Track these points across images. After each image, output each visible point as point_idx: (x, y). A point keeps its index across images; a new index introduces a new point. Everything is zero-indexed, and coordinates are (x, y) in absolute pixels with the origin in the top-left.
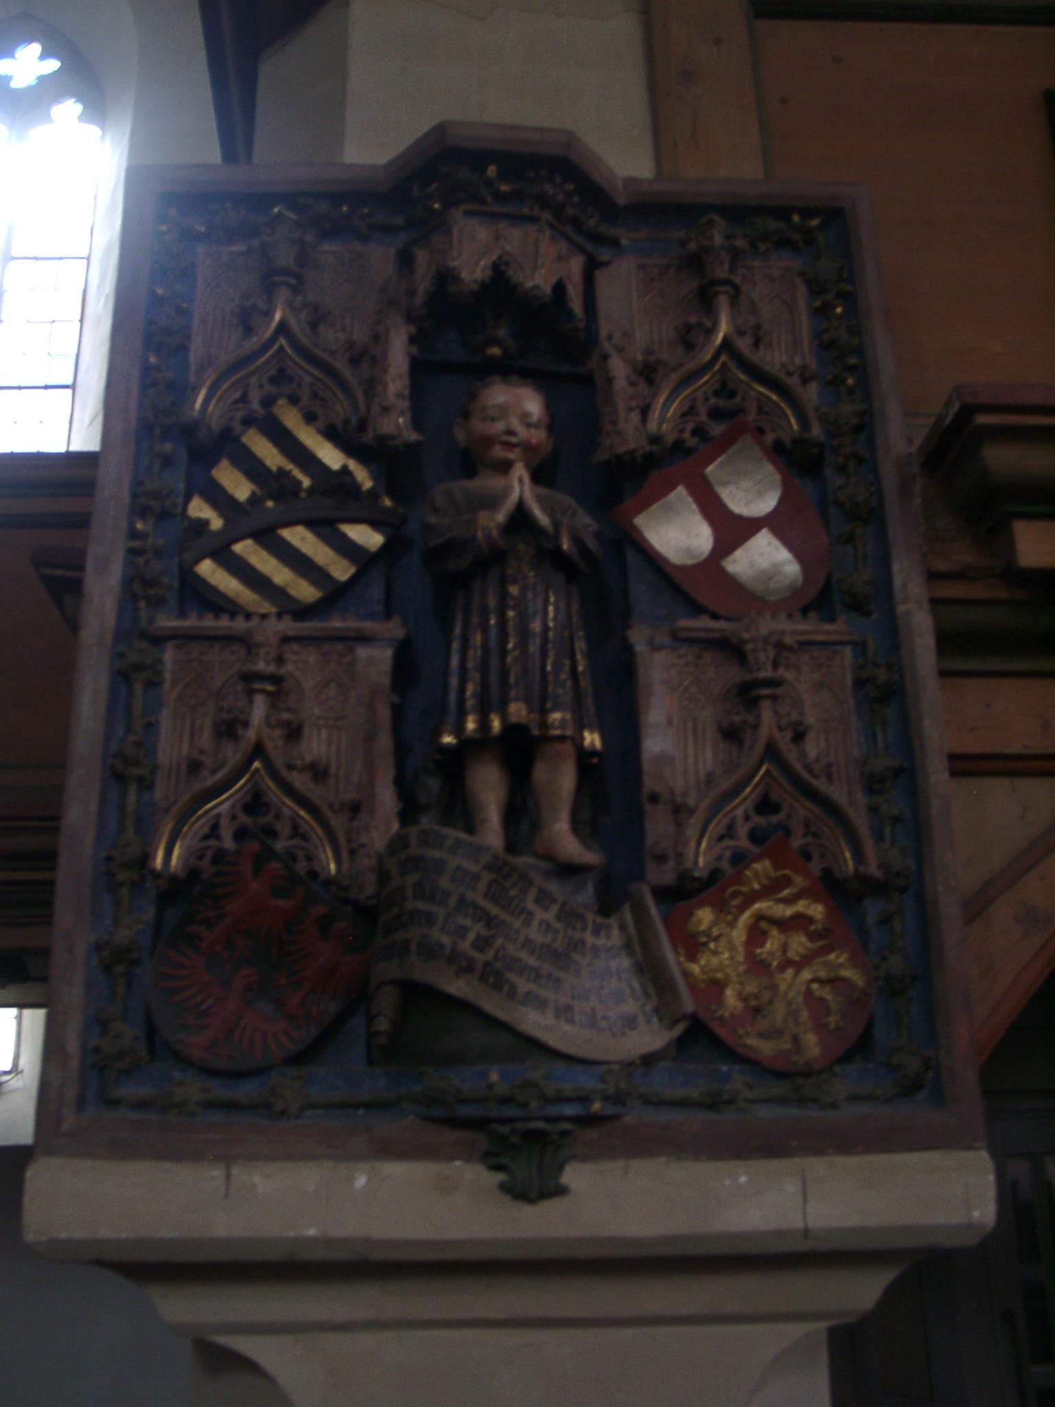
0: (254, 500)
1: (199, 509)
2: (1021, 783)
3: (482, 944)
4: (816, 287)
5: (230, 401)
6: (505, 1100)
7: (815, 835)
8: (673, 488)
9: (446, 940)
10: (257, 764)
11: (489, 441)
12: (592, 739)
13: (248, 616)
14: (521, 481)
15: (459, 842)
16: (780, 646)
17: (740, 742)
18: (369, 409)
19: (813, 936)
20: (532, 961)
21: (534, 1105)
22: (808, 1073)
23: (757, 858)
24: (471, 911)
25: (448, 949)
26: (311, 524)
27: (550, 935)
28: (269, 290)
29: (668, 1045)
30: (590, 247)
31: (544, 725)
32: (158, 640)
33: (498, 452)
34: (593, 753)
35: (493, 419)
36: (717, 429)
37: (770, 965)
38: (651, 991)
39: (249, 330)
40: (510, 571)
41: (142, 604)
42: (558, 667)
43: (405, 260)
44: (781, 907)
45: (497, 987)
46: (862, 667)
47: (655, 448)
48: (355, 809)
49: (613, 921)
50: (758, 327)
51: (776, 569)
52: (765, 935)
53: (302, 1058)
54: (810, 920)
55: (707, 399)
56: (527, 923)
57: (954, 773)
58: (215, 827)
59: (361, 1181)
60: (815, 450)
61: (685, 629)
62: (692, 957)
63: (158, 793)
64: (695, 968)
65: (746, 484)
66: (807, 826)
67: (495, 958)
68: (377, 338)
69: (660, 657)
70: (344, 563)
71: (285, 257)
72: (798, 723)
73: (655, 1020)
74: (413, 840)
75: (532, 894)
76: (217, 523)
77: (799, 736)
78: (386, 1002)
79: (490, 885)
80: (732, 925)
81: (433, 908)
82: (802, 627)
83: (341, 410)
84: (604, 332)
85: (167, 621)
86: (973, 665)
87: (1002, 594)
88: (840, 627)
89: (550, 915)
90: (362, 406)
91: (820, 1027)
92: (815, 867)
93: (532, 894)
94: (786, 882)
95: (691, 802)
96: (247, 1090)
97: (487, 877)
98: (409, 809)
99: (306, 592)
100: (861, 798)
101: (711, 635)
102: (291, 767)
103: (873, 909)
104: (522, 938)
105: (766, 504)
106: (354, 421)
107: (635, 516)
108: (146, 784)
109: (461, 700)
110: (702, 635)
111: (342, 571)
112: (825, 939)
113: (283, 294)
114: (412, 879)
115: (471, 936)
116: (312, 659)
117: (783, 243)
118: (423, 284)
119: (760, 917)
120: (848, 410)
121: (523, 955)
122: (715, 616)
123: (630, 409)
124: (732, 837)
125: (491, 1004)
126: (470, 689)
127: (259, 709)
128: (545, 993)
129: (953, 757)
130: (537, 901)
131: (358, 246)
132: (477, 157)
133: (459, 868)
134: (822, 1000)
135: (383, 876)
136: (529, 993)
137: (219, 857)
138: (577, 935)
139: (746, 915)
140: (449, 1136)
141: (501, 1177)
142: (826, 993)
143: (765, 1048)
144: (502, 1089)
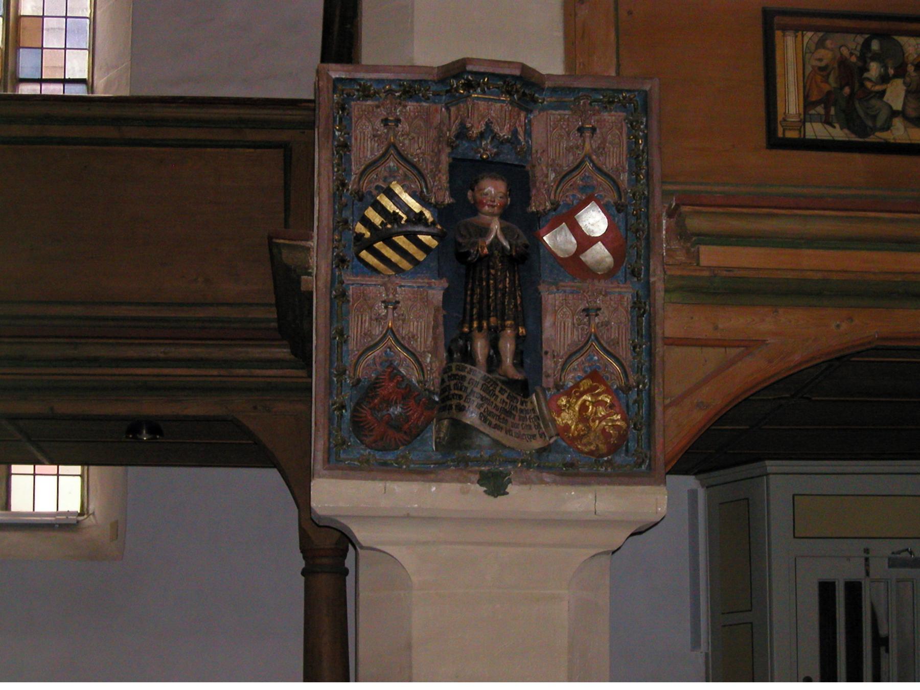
0: (382, 223)
1: (360, 228)
42: (509, 303)
54: (607, 402)
56: (496, 399)
59: (434, 489)
67: (484, 411)
70: (421, 253)
75: (498, 389)
76: (368, 234)
81: (460, 393)
89: (505, 397)
93: (498, 389)
104: (494, 405)
109: (471, 316)
111: (420, 256)
114: (452, 383)
119: (585, 401)
121: (494, 411)
126: (475, 311)
128: (502, 425)
130: (499, 392)
136: (496, 424)
139: (579, 402)
141: (485, 489)
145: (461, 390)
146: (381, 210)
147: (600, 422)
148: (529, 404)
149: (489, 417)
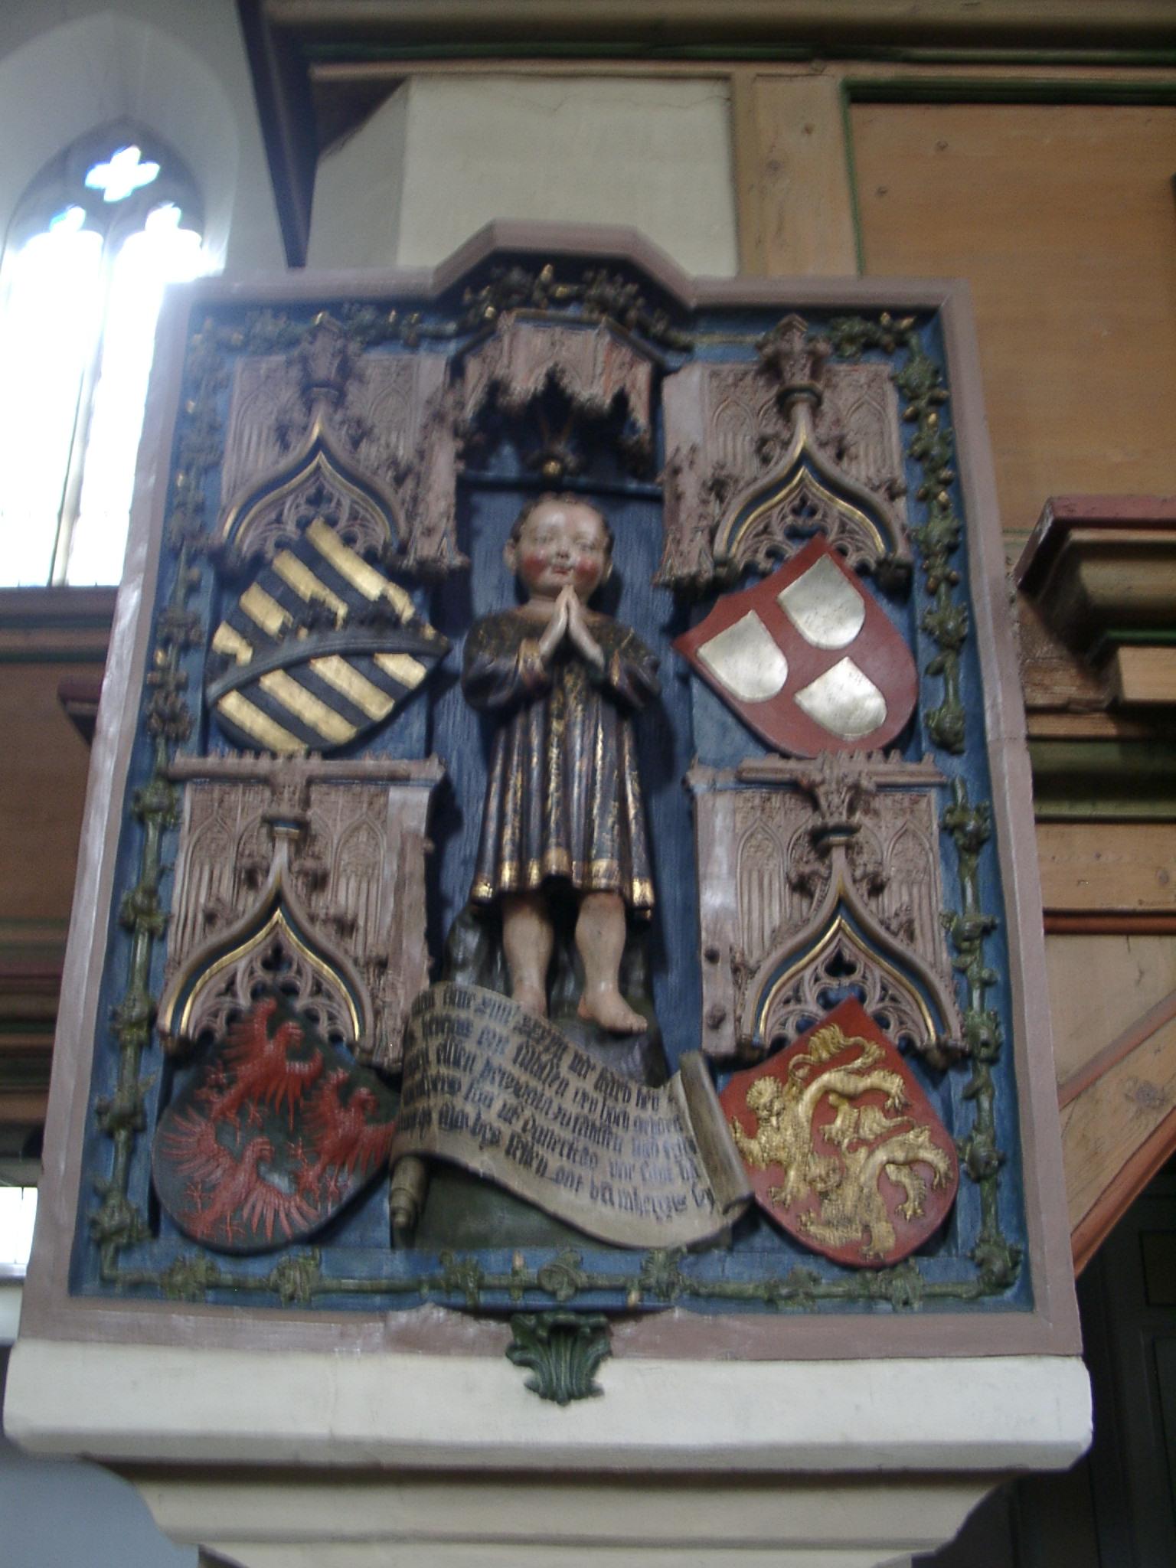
0: (284, 630)
1: (226, 639)
2: (1134, 941)
3: (508, 1114)
4: (907, 393)
5: (265, 521)
6: (528, 1289)
7: (893, 999)
8: (746, 613)
9: (470, 1110)
10: (278, 914)
11: (539, 565)
12: (641, 891)
14: (568, 608)
16: (856, 789)
17: (810, 895)
18: (411, 532)
19: (887, 1113)
20: (566, 1135)
21: (562, 1294)
22: (878, 1267)
23: (825, 1024)
24: (497, 1079)
26: (347, 655)
27: (587, 1106)
28: (309, 407)
29: (723, 1231)
30: (657, 353)
31: (587, 875)
32: (175, 781)
33: (549, 577)
34: (644, 907)
35: (545, 540)
36: (792, 550)
37: (839, 1144)
38: (703, 1170)
39: (285, 446)
40: (554, 706)
41: (161, 742)
43: (457, 369)
44: (854, 1078)
45: (526, 1162)
46: (951, 811)
47: (723, 571)
48: (382, 965)
49: (662, 1093)
50: (841, 439)
51: (856, 704)
52: (835, 1109)
53: (324, 1235)
54: (887, 1095)
55: (784, 518)
56: (561, 1092)
57: (1049, 931)
58: (231, 983)
60: (902, 572)
61: (751, 770)
62: (751, 1134)
63: (170, 946)
64: (754, 1146)
65: (825, 610)
66: (884, 988)
67: (524, 1130)
68: (421, 454)
69: (723, 803)
71: (325, 368)
72: (876, 875)
73: (706, 1201)
75: (567, 1060)
76: (245, 655)
77: (877, 888)
78: (407, 1179)
79: (519, 1050)
80: (797, 1098)
81: (457, 1074)
82: (882, 767)
83: (380, 533)
84: (670, 450)
85: (185, 760)
86: (1084, 810)
87: (1110, 730)
88: (929, 766)
89: (588, 1084)
91: (895, 1213)
92: (893, 1034)
93: (567, 1060)
94: (858, 1051)
95: (752, 962)
96: (257, 1270)
98: (442, 966)
99: (338, 729)
100: (945, 958)
101: (779, 777)
102: (312, 918)
103: (957, 1082)
104: (555, 1108)
105: (846, 633)
106: (395, 546)
107: (700, 646)
108: (157, 936)
110: (770, 776)
111: (378, 706)
112: (904, 1115)
113: (320, 412)
114: (435, 1042)
115: (497, 1105)
116: (341, 802)
117: (870, 346)
118: (473, 395)
120: (938, 528)
121: (556, 1128)
122: (785, 756)
123: (696, 529)
124: (798, 1000)
125: (518, 1181)
127: (281, 856)
128: (579, 1170)
129: (1048, 914)
131: (406, 356)
132: (532, 261)
134: (898, 1185)
135: (408, 1039)
136: (562, 1170)
137: (233, 1017)
139: (813, 1089)
140: (472, 1328)
141: (527, 1374)
142: (904, 1177)
143: (832, 1238)
144: (530, 1274)
145: (457, 1063)
146: (287, 598)
147: (871, 1153)
148: (664, 1102)
149: (537, 1148)
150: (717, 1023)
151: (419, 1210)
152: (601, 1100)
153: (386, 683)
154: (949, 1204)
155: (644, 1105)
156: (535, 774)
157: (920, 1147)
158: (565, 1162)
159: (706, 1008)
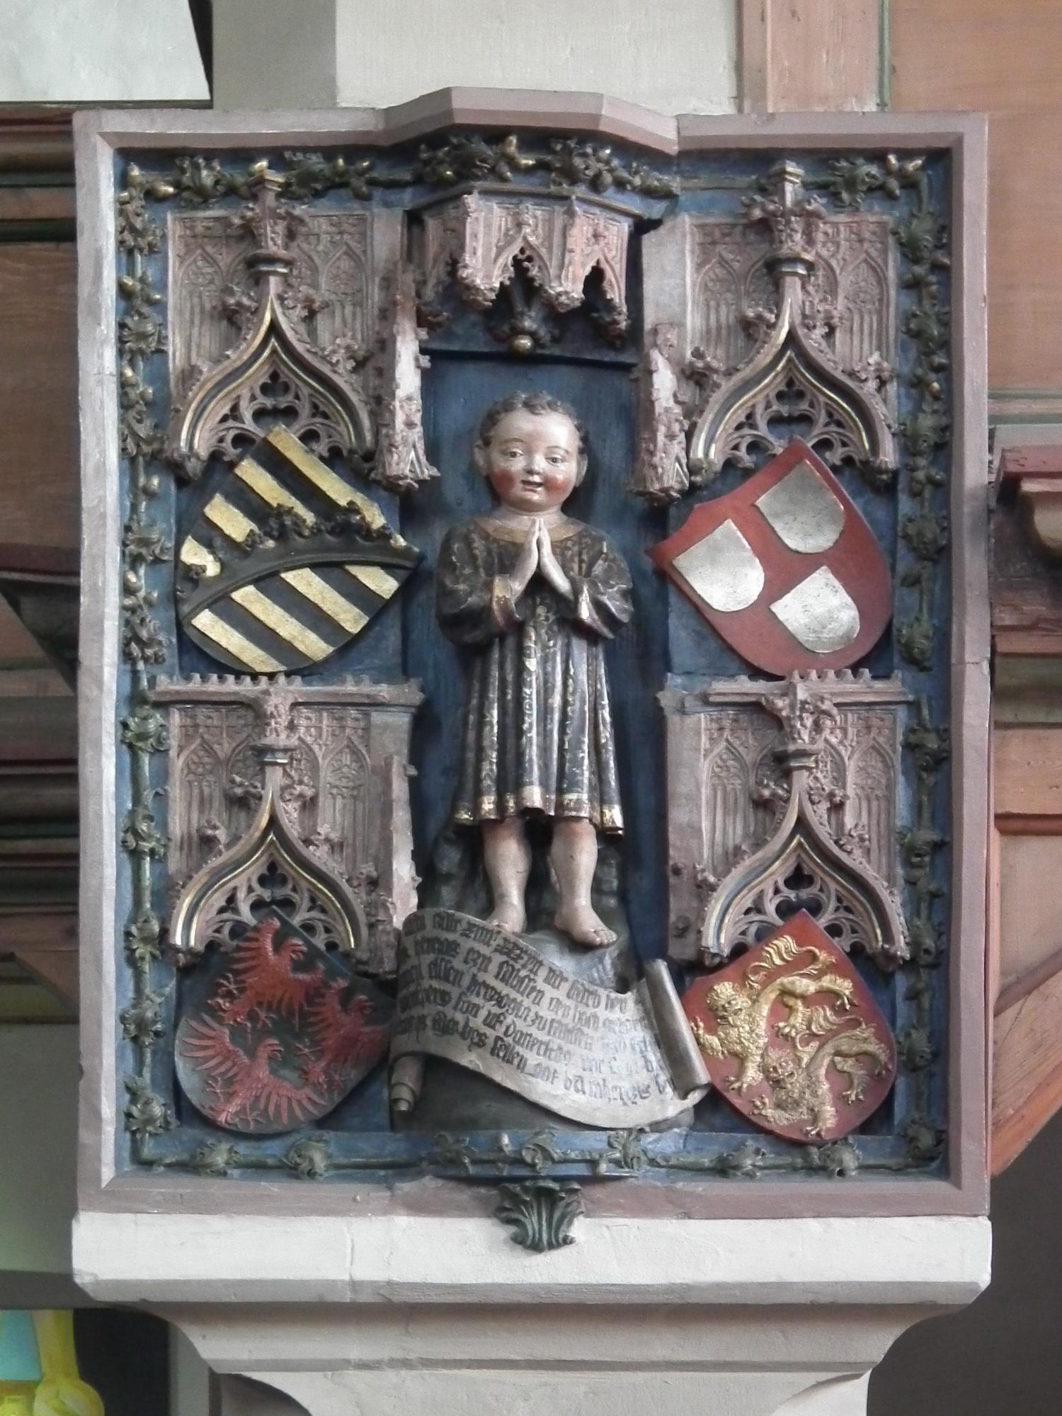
9: (459, 1017)
10: (271, 836)
13: (255, 676)
15: (471, 926)
19: (839, 1011)
22: (820, 1143)
25: (462, 1023)
44: (805, 981)
54: (838, 995)
56: (537, 1002)
58: (231, 900)
66: (839, 900)
67: (506, 1033)
74: (429, 923)
75: (543, 973)
85: (168, 684)
90: (368, 437)
97: (498, 959)
99: (314, 646)
104: (532, 1015)
109: (478, 780)
111: (351, 619)
114: (428, 958)
115: (483, 1013)
121: (534, 1031)
125: (501, 1075)
128: (553, 1065)
130: (547, 980)
133: (471, 950)
135: (401, 954)
137: (239, 930)
138: (590, 1011)
145: (446, 979)
150: (682, 933)
151: (419, 1102)
152: (573, 1007)
153: (358, 595)
154: (886, 1093)
155: (612, 1006)
156: (511, 706)
157: (865, 1040)
158: (541, 1059)
159: (673, 918)
